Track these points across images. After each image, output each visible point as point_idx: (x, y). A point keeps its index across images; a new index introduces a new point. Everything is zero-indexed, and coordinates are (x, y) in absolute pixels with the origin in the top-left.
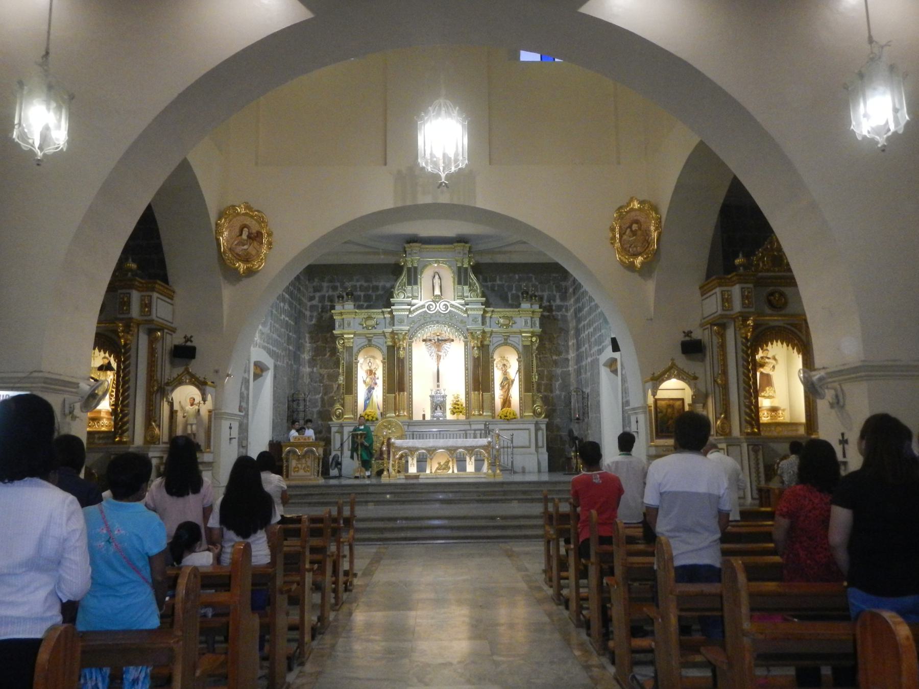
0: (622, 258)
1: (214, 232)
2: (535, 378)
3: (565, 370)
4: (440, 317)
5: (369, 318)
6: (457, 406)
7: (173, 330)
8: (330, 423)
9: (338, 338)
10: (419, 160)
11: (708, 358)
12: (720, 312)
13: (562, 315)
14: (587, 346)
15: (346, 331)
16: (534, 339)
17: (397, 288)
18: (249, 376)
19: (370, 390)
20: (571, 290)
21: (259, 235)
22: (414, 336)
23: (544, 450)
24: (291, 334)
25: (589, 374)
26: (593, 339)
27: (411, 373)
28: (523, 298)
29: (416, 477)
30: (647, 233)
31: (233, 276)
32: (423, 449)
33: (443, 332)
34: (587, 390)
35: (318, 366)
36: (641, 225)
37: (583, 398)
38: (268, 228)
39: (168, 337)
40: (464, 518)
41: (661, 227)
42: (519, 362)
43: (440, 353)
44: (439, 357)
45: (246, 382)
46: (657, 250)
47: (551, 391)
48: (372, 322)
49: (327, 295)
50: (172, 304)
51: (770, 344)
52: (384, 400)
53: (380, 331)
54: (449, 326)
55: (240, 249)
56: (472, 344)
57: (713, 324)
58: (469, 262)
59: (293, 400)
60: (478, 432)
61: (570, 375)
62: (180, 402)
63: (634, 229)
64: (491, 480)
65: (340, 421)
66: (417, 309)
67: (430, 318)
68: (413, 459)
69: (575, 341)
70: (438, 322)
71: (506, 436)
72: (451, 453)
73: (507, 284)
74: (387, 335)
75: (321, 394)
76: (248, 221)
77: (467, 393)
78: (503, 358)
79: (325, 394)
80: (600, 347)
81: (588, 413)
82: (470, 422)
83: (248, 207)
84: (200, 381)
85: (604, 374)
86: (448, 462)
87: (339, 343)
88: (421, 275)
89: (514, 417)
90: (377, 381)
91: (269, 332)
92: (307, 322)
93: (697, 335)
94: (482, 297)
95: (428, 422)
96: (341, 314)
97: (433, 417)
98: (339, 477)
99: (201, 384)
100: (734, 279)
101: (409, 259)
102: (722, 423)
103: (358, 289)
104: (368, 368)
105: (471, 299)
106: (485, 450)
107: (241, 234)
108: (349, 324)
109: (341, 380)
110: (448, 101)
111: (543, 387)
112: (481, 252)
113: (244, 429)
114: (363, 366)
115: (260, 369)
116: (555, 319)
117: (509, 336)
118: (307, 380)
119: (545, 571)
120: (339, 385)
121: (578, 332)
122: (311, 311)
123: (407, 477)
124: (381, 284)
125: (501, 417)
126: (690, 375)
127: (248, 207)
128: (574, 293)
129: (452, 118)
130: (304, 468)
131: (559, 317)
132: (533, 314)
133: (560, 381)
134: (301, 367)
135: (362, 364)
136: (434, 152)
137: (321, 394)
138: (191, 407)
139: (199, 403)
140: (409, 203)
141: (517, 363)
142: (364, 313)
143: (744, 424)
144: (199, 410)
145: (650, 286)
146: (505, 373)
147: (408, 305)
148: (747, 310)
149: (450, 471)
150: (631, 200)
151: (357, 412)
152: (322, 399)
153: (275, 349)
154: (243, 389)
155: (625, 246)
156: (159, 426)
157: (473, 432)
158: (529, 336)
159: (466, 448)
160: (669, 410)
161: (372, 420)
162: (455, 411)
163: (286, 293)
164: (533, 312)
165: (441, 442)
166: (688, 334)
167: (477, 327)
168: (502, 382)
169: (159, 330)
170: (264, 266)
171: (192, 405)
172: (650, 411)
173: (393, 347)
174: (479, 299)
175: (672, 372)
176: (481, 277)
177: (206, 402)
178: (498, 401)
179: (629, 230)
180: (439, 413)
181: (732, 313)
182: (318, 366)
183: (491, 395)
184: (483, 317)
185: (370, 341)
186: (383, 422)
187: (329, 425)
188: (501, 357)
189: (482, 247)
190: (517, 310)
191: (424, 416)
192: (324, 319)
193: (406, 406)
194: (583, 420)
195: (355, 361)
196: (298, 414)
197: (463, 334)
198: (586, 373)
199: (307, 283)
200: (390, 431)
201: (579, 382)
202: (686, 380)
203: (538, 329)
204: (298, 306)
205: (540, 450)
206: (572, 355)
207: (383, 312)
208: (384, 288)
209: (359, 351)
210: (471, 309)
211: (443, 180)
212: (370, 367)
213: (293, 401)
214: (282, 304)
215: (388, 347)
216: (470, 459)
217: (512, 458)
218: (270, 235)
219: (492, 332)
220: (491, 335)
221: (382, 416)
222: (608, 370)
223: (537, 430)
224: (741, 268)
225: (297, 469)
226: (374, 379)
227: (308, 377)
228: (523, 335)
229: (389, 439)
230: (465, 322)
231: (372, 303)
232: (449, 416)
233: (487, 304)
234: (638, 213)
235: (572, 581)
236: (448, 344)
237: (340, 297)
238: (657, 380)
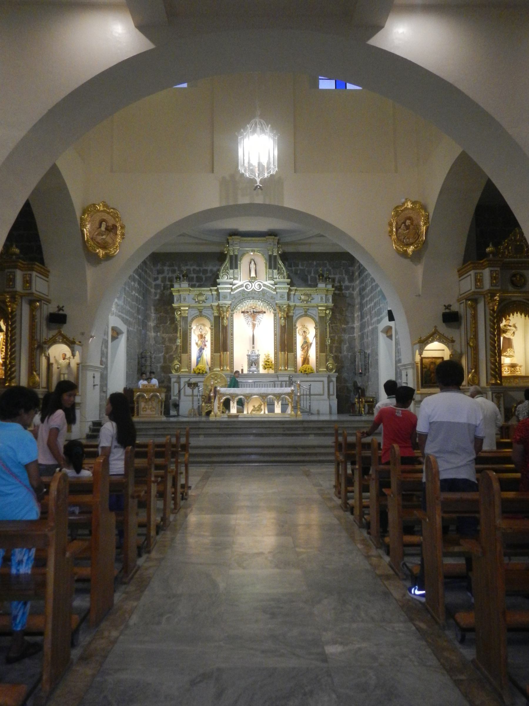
0: (398, 247)
1: (79, 224)
2: (328, 342)
3: (351, 336)
4: (255, 294)
5: (201, 294)
6: (268, 363)
7: (49, 301)
8: (170, 375)
9: (177, 310)
10: (240, 168)
11: (463, 327)
12: (473, 289)
13: (349, 293)
14: (368, 317)
16: (328, 312)
17: (221, 271)
18: (108, 337)
19: (201, 350)
20: (357, 274)
21: (114, 227)
22: (234, 308)
23: (335, 397)
24: (140, 306)
25: (370, 339)
26: (373, 312)
27: (233, 337)
28: (319, 279)
29: (237, 416)
30: (417, 227)
31: (95, 260)
32: (241, 395)
33: (258, 306)
34: (368, 351)
35: (161, 332)
36: (413, 221)
37: (365, 357)
38: (121, 222)
39: (45, 306)
40: (273, 447)
41: (429, 222)
42: (316, 329)
43: (255, 322)
44: (254, 325)
45: (105, 342)
46: (425, 240)
47: (340, 353)
48: (203, 298)
49: (168, 276)
51: (511, 315)
53: (209, 305)
55: (99, 238)
56: (280, 315)
57: (467, 300)
58: (278, 251)
59: (142, 357)
60: (284, 383)
61: (355, 340)
62: (55, 357)
63: (407, 224)
64: (293, 419)
65: (179, 373)
66: (237, 288)
67: (247, 295)
68: (234, 403)
69: (359, 313)
70: (253, 298)
71: (305, 386)
72: (263, 398)
73: (306, 269)
74: (214, 308)
75: (163, 353)
76: (106, 217)
77: (276, 353)
78: (304, 326)
79: (167, 353)
80: (379, 318)
81: (369, 369)
82: (277, 375)
83: (105, 205)
84: (70, 340)
85: (382, 338)
86: (261, 405)
87: (177, 313)
88: (240, 261)
89: (311, 372)
90: (206, 343)
91: (123, 304)
92: (152, 297)
93: (455, 308)
94: (288, 278)
95: (245, 375)
96: (179, 291)
97: (249, 371)
98: (178, 415)
99: (71, 343)
100: (485, 263)
101: (231, 248)
102: (473, 376)
103: (192, 272)
104: (200, 333)
105: (279, 280)
106: (289, 396)
107: (100, 226)
108: (185, 299)
110: (262, 121)
111: (334, 349)
112: (287, 244)
113: (104, 378)
114: (196, 332)
115: (116, 333)
116: (344, 296)
118: (152, 342)
119: (335, 487)
120: (177, 346)
121: (362, 306)
122: (155, 289)
123: (230, 416)
124: (209, 268)
125: (301, 372)
126: (449, 339)
127: (105, 205)
128: (360, 275)
129: (265, 134)
130: (151, 409)
131: (348, 295)
132: (327, 292)
133: (348, 345)
134: (148, 332)
135: (195, 330)
136: (251, 162)
137: (163, 353)
138: (64, 361)
139: (70, 358)
140: (231, 203)
141: (314, 330)
142: (197, 290)
143: (490, 377)
144: (69, 363)
145: (419, 270)
146: (305, 338)
147: (230, 285)
148: (495, 288)
149: (262, 412)
150: (406, 201)
151: (191, 367)
152: (164, 358)
153: (127, 317)
155: (400, 238)
157: (280, 383)
158: (324, 310)
159: (274, 395)
160: (432, 366)
161: (202, 373)
162: (266, 366)
163: (136, 274)
164: (327, 291)
165: (255, 390)
166: (448, 307)
168: (303, 345)
169: (38, 301)
170: (118, 252)
171: (64, 359)
172: (418, 366)
173: (219, 317)
174: (285, 280)
175: (435, 337)
176: (287, 263)
177: (75, 357)
178: (300, 359)
179: (404, 224)
180: (253, 368)
181: (483, 290)
182: (161, 332)
184: (289, 295)
185: (201, 312)
186: (211, 375)
187: (169, 377)
188: (302, 326)
189: (288, 239)
190: (315, 289)
191: (242, 370)
192: (165, 295)
193: (228, 363)
194: (365, 375)
195: (189, 327)
196: (146, 368)
197: (272, 308)
198: (367, 338)
199: (152, 267)
200: (216, 382)
201: (362, 345)
202: (445, 342)
203: (330, 304)
204: (145, 284)
205: (331, 397)
206: (357, 324)
207: (211, 290)
208: (211, 271)
209: (192, 320)
210: (279, 288)
211: (258, 184)
212: (201, 332)
213: (142, 358)
214: (133, 283)
215: (215, 317)
216: (278, 403)
217: (310, 403)
218: (123, 227)
219: (295, 306)
220: (294, 308)
221: (210, 370)
222: (385, 335)
223: (329, 381)
224: (491, 255)
225: (145, 409)
226: (204, 342)
227: (153, 340)
228: (320, 308)
229: (216, 388)
230: (275, 298)
231: (202, 283)
232: (262, 371)
233: (291, 284)
234: (411, 211)
235: (356, 494)
236: (261, 315)
237: (178, 278)
238: (423, 342)
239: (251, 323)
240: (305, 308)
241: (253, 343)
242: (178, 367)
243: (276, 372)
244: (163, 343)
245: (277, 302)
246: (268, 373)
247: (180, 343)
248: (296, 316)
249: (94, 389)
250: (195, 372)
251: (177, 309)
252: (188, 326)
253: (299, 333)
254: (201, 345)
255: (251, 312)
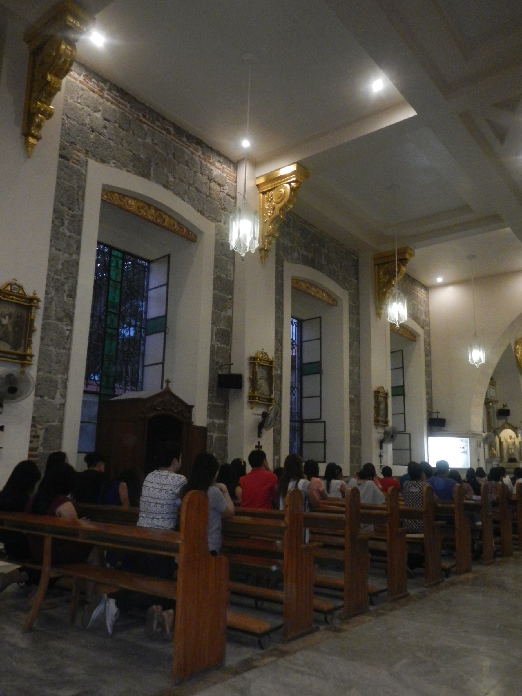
7: (497, 402)
50: (495, 389)
62: (505, 438)
99: (515, 429)
139: (514, 438)
144: (514, 442)
156: (495, 449)
171: (511, 439)
177: (518, 438)
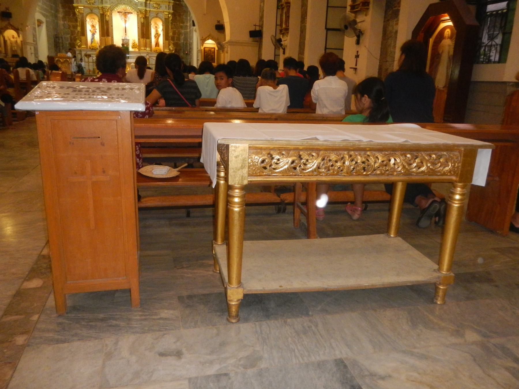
2: (171, 34)
3: (185, 31)
8: (75, 49)
15: (78, 5)
16: (170, 16)
18: (35, 25)
19: (93, 34)
22: (113, 10)
24: (52, 5)
34: (191, 41)
37: (190, 45)
42: (163, 26)
43: (126, 19)
44: (125, 21)
45: (34, 29)
47: (179, 41)
52: (100, 40)
53: (96, 6)
54: (130, 6)
56: (141, 16)
61: (188, 33)
62: (8, 37)
65: (80, 49)
70: (124, 4)
74: (100, 8)
75: (70, 35)
77: (139, 39)
78: (156, 23)
79: (72, 34)
82: (140, 52)
87: (76, 10)
90: (96, 31)
99: (17, 30)
104: (92, 24)
109: (79, 29)
113: (36, 50)
115: (40, 23)
117: (158, 13)
118: (62, 27)
120: (78, 31)
130: (65, 67)
135: (88, 22)
137: (70, 35)
138: (13, 39)
144: (17, 41)
146: (157, 31)
151: (88, 45)
152: (71, 38)
154: (34, 32)
160: (209, 52)
161: (95, 49)
162: (133, 47)
164: (169, 2)
166: (219, 22)
167: (143, 8)
171: (13, 38)
172: (202, 52)
173: (103, 14)
177: (20, 38)
183: (150, 41)
185: (91, 11)
194: (189, 54)
195: (85, 20)
203: (171, 11)
209: (87, 15)
212: (93, 23)
213: (56, 38)
215: (101, 14)
219: (150, 11)
226: (95, 29)
238: (203, 40)
239: (124, 20)
240: (156, 12)
241: (126, 32)
242: (79, 44)
243: (139, 50)
244: (69, 28)
245: (138, 7)
246: (135, 51)
247: (80, 29)
248: (151, 17)
249: (31, 55)
250: (90, 48)
251: (76, 7)
252: (84, 19)
253: (153, 27)
254: (93, 31)
255: (123, 12)
